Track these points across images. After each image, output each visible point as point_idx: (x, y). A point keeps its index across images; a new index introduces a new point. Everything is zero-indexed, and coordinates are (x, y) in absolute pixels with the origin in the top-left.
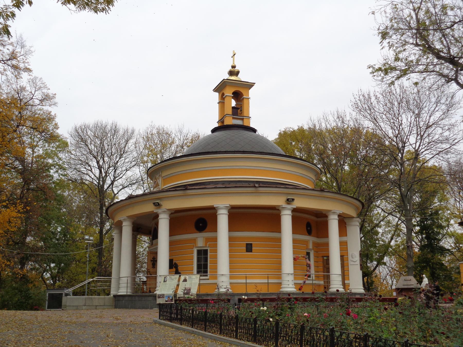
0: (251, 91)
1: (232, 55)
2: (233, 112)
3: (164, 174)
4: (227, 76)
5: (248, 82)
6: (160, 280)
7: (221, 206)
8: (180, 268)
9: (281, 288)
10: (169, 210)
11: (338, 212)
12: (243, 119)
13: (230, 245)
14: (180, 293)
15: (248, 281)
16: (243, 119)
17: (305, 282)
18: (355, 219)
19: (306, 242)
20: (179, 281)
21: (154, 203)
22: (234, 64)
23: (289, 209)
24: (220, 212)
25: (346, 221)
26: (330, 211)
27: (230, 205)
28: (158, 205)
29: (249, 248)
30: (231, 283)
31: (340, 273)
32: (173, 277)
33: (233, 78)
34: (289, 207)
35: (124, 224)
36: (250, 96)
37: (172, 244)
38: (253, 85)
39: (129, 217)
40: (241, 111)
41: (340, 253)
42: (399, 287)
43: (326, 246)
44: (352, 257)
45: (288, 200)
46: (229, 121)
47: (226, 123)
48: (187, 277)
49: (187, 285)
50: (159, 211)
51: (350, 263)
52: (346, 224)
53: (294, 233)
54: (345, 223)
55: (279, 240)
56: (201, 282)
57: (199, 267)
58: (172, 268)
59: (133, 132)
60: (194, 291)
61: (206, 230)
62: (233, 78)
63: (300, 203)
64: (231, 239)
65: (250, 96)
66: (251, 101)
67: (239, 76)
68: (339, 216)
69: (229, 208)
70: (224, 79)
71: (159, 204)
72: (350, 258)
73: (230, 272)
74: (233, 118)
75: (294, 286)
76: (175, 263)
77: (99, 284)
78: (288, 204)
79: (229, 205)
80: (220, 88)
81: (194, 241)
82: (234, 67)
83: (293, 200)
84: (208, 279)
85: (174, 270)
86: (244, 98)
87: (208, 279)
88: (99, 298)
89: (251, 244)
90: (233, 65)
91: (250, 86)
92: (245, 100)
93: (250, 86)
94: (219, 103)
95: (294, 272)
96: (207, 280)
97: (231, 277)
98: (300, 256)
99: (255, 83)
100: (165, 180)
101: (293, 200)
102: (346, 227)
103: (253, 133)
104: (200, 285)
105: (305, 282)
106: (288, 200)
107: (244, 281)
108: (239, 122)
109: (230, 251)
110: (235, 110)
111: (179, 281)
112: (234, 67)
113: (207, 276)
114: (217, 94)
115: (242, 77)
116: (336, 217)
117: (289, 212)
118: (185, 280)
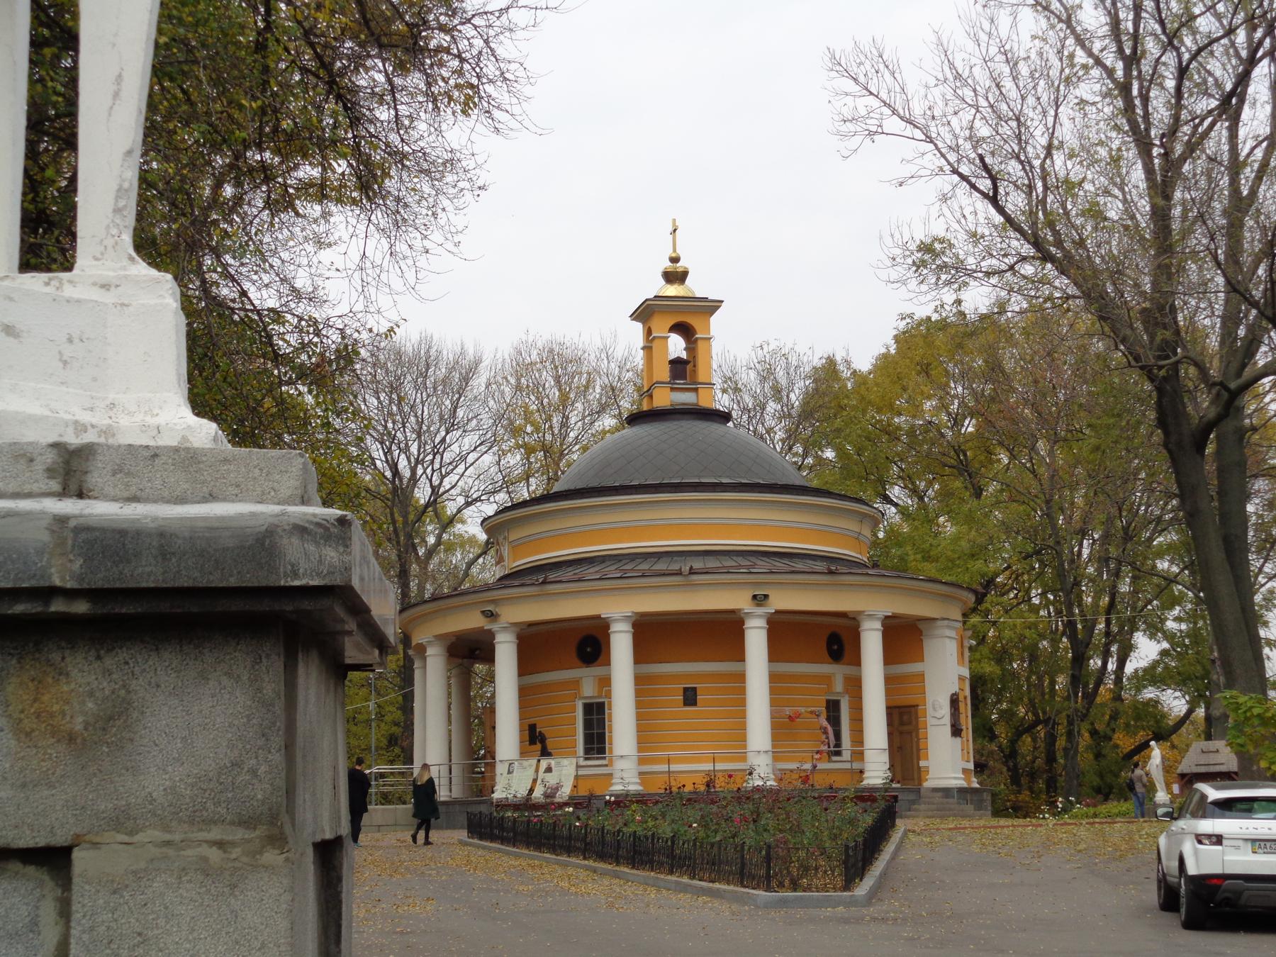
0: (715, 320)
1: (671, 229)
2: (672, 371)
3: (514, 536)
4: (656, 287)
5: (705, 299)
6: (501, 769)
7: (616, 616)
8: (549, 743)
9: (612, 785)
11: (881, 615)
12: (696, 390)
13: (639, 693)
14: (538, 794)
15: (674, 767)
16: (696, 390)
17: (815, 767)
18: (939, 623)
19: (828, 679)
20: (537, 771)
21: (483, 612)
22: (675, 250)
23: (760, 616)
24: (615, 627)
25: (920, 627)
27: (636, 613)
28: (491, 615)
29: (690, 697)
30: (641, 774)
31: (885, 745)
32: (525, 763)
33: (672, 290)
34: (761, 610)
35: (430, 651)
36: (712, 333)
37: (525, 694)
38: (719, 307)
39: (439, 637)
40: (695, 366)
41: (887, 701)
42: (1185, 772)
43: (855, 686)
44: (935, 709)
45: (755, 597)
46: (664, 398)
48: (553, 763)
49: (552, 779)
50: (494, 627)
51: (930, 721)
54: (921, 633)
55: (741, 678)
56: (580, 773)
57: (589, 739)
58: (535, 743)
59: (477, 363)
60: (566, 792)
61: (599, 661)
62: (672, 290)
64: (640, 680)
65: (713, 332)
67: (687, 282)
69: (634, 619)
70: (647, 300)
71: (492, 615)
72: (930, 712)
73: (640, 749)
74: (672, 389)
75: (638, 781)
76: (540, 732)
77: (391, 779)
78: (759, 605)
80: (644, 313)
81: (576, 684)
82: (675, 260)
83: (766, 596)
84: (606, 766)
86: (697, 339)
87: (606, 766)
88: (384, 810)
89: (695, 689)
90: (674, 255)
91: (710, 307)
92: (700, 344)
93: (710, 307)
94: (643, 348)
95: (774, 746)
96: (594, 767)
97: (642, 761)
98: (803, 710)
100: (517, 547)
101: (766, 596)
102: (922, 640)
103: (715, 428)
104: (577, 777)
105: (815, 767)
106: (755, 597)
107: (664, 768)
108: (686, 398)
109: (639, 705)
110: (678, 366)
111: (537, 771)
112: (675, 260)
113: (604, 758)
114: (638, 327)
115: (696, 286)
116: (878, 625)
117: (762, 623)
118: (549, 770)
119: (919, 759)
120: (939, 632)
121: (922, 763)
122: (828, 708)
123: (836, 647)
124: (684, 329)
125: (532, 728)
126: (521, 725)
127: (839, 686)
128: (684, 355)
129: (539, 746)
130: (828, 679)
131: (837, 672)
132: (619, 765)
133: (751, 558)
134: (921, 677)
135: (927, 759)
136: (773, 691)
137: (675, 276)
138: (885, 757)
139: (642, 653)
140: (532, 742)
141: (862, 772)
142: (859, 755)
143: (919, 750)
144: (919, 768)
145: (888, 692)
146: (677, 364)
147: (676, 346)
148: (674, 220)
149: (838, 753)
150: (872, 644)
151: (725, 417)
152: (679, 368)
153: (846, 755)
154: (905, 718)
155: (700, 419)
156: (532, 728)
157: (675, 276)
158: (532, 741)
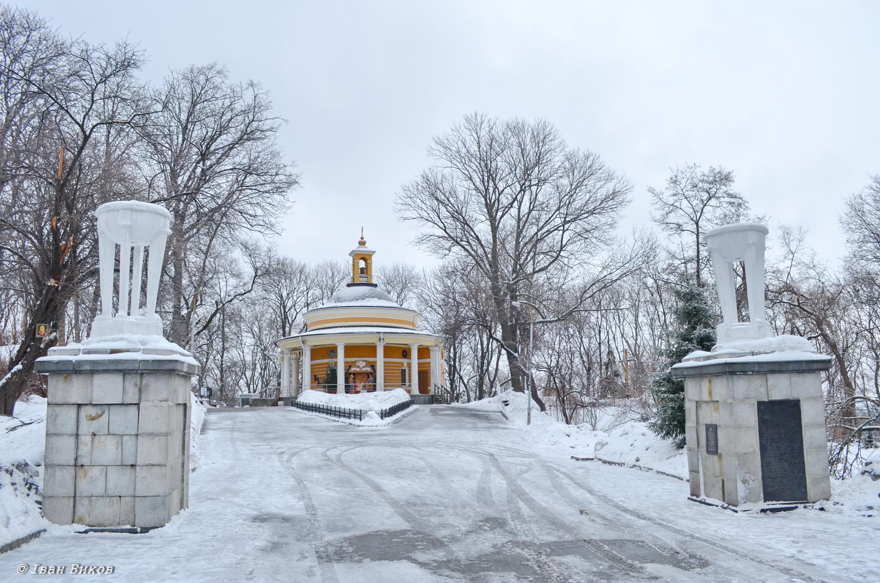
4: (355, 246)
19: (402, 364)
112: (362, 238)
115: (369, 247)
124: (364, 259)
125: (315, 376)
126: (311, 376)
127: (405, 365)
130: (402, 364)
131: (405, 361)
134: (429, 363)
137: (362, 243)
139: (346, 355)
140: (315, 380)
142: (410, 386)
145: (419, 367)
147: (362, 264)
150: (414, 354)
151: (376, 286)
152: (363, 271)
153: (407, 383)
156: (315, 376)
157: (362, 243)
158: (315, 380)
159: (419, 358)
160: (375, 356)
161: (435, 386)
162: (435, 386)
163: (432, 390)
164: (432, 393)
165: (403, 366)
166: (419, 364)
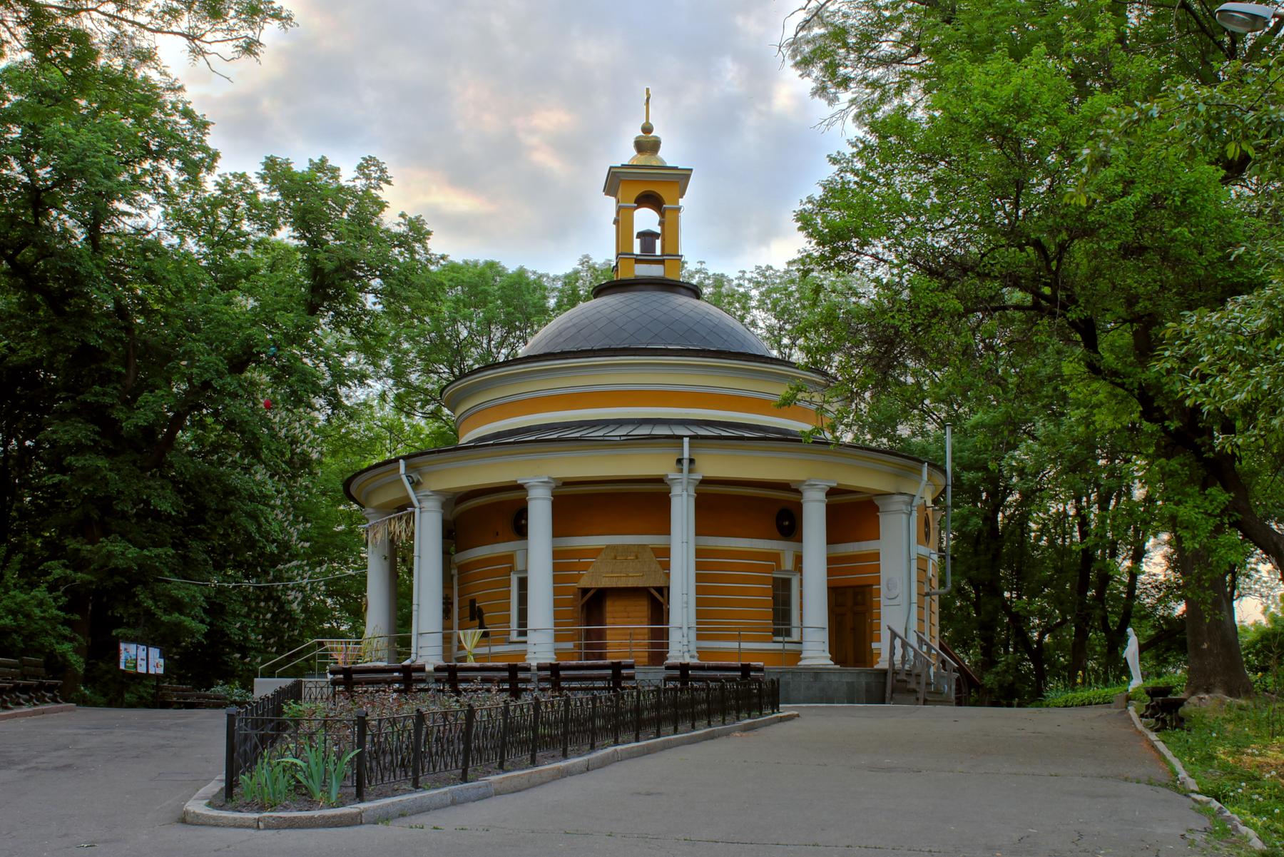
4: (626, 154)
5: (676, 168)
10: (436, 492)
12: (661, 262)
13: (556, 567)
19: (775, 557)
24: (533, 494)
25: (876, 502)
26: (802, 482)
33: (644, 160)
38: (688, 177)
47: (622, 275)
51: (883, 600)
52: (878, 510)
53: (699, 533)
54: (877, 509)
55: (664, 553)
63: (719, 465)
66: (682, 215)
67: (661, 153)
68: (831, 492)
69: (553, 485)
74: (638, 261)
79: (549, 478)
85: (477, 622)
91: (680, 179)
92: (668, 214)
93: (680, 179)
99: (691, 170)
108: (655, 271)
112: (647, 129)
116: (822, 496)
119: (872, 641)
120: (895, 507)
121: (874, 645)
122: (775, 587)
123: (787, 523)
124: (650, 200)
125: (473, 602)
127: (788, 564)
128: (658, 230)
129: (477, 622)
130: (775, 557)
132: (531, 637)
133: (692, 428)
134: (876, 556)
135: (879, 641)
136: (699, 566)
138: (824, 636)
139: (561, 525)
140: (472, 618)
141: (801, 652)
143: (872, 631)
144: (872, 650)
146: (648, 237)
147: (646, 219)
148: (648, 90)
149: (788, 633)
153: (795, 636)
154: (859, 597)
155: (662, 290)
159: (832, 538)
160: (666, 531)
161: (894, 635)
162: (894, 635)
163: (884, 653)
164: (883, 664)
165: (779, 564)
166: (831, 560)
